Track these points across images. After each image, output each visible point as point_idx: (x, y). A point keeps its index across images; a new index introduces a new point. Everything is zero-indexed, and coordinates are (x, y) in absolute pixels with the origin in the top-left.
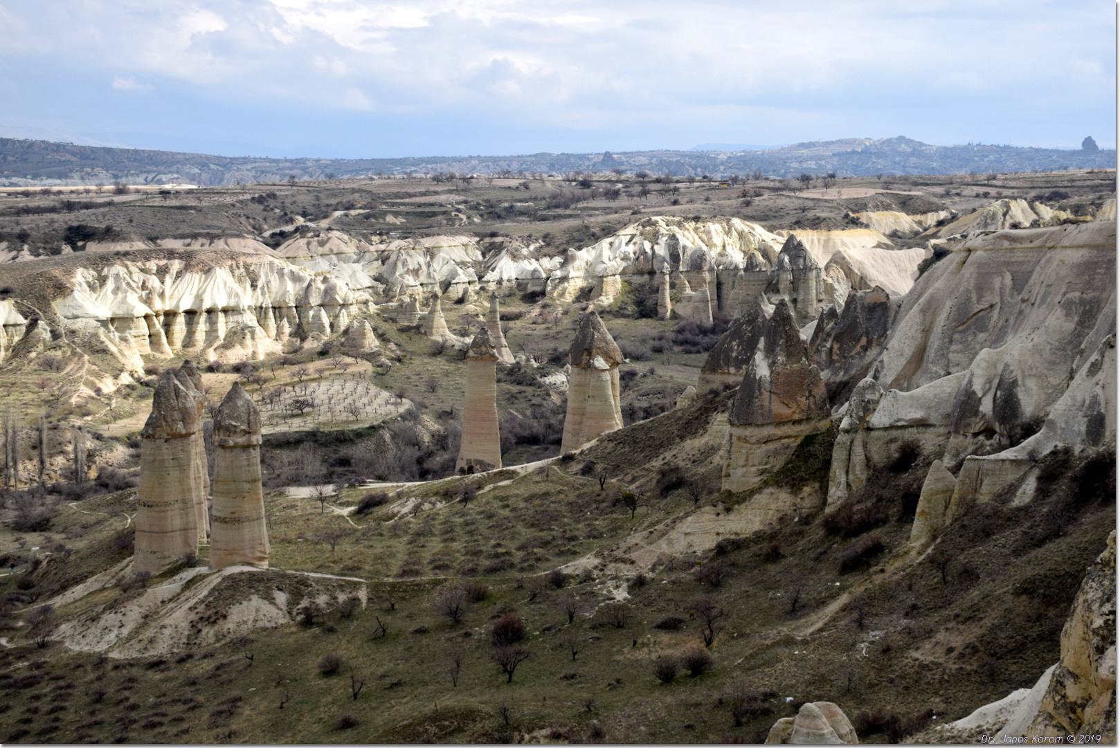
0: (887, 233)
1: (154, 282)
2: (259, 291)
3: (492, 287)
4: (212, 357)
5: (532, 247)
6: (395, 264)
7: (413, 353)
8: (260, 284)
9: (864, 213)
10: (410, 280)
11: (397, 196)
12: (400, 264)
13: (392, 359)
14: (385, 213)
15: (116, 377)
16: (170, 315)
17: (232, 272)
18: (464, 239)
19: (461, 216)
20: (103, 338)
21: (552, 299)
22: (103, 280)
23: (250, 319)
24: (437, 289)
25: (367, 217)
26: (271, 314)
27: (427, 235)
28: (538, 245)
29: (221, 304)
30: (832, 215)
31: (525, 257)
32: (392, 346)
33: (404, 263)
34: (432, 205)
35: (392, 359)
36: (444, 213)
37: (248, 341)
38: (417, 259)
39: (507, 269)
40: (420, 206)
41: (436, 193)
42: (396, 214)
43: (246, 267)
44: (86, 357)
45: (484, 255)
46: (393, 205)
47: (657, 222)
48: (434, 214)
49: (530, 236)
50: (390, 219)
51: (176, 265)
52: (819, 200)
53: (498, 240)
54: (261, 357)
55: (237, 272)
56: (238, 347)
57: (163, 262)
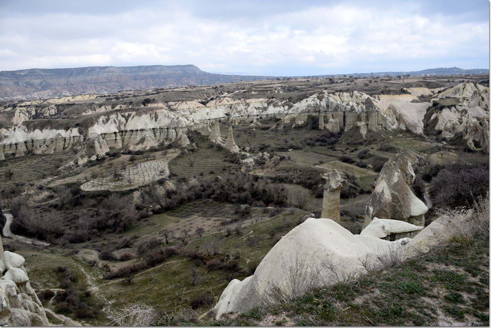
0: (420, 95)
1: (123, 120)
2: (157, 122)
3: (264, 117)
4: (131, 148)
5: (283, 102)
6: (233, 110)
7: (201, 147)
8: (158, 120)
9: (411, 88)
10: (237, 115)
11: (260, 85)
12: (234, 109)
13: (189, 150)
14: (252, 91)
15: (89, 157)
16: (126, 131)
17: (150, 115)
18: (262, 100)
19: (276, 91)
20: (96, 142)
21: (282, 122)
22: (108, 120)
23: (149, 134)
24: (246, 118)
25: (244, 92)
26: (159, 131)
27: (249, 98)
28: (285, 101)
29: (139, 129)
30: (396, 89)
31: (279, 106)
32: (194, 144)
33: (237, 108)
34: (270, 88)
35: (189, 150)
36: (270, 90)
37: (145, 143)
38: (241, 107)
39: (272, 110)
40: (265, 88)
41: (274, 84)
42: (255, 91)
43: (156, 113)
44: (85, 149)
45: (268, 105)
46: (257, 88)
47: (324, 92)
48: (267, 91)
49: (283, 98)
50: (253, 93)
51: (134, 113)
52: (394, 83)
53: (274, 99)
54: (148, 148)
55: (152, 116)
56: (141, 144)
57: (130, 113)
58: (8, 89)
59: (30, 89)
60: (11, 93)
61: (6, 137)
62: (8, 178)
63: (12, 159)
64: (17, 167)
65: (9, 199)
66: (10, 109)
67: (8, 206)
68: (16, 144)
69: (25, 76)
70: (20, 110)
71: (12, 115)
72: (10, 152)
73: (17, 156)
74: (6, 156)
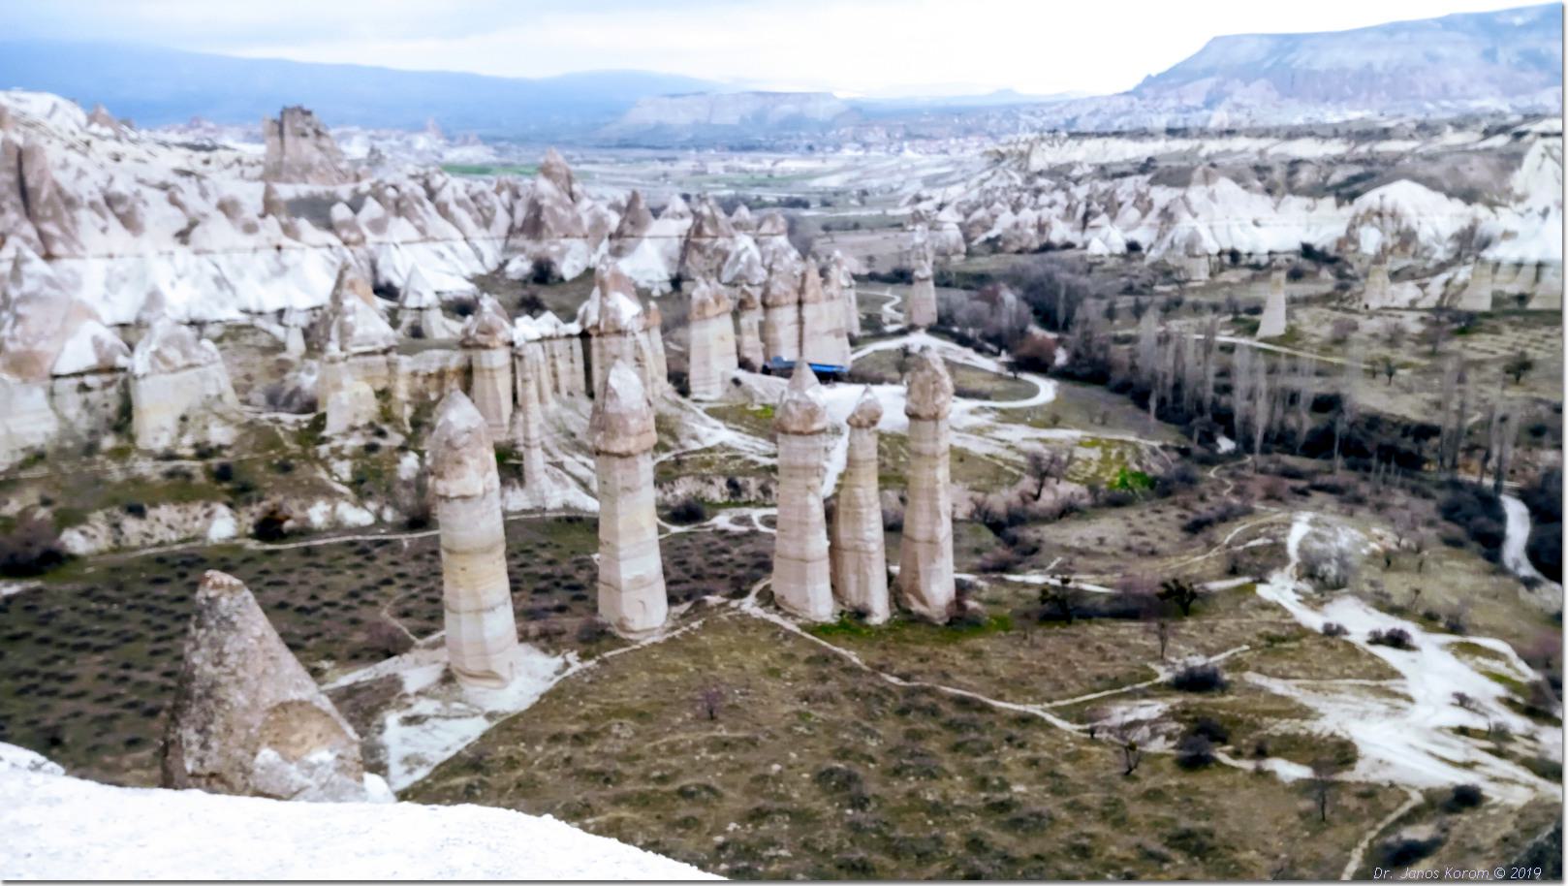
58: (1456, 76)
59: (1531, 77)
60: (1463, 88)
61: (1507, 235)
62: (1512, 376)
63: (1515, 313)
64: (1535, 344)
65: (1519, 451)
66: (1500, 141)
67: (1513, 472)
68: (1540, 266)
69: (1528, 27)
70: (1547, 148)
71: (1511, 160)
72: (1513, 289)
73: (1533, 305)
74: (1497, 300)
